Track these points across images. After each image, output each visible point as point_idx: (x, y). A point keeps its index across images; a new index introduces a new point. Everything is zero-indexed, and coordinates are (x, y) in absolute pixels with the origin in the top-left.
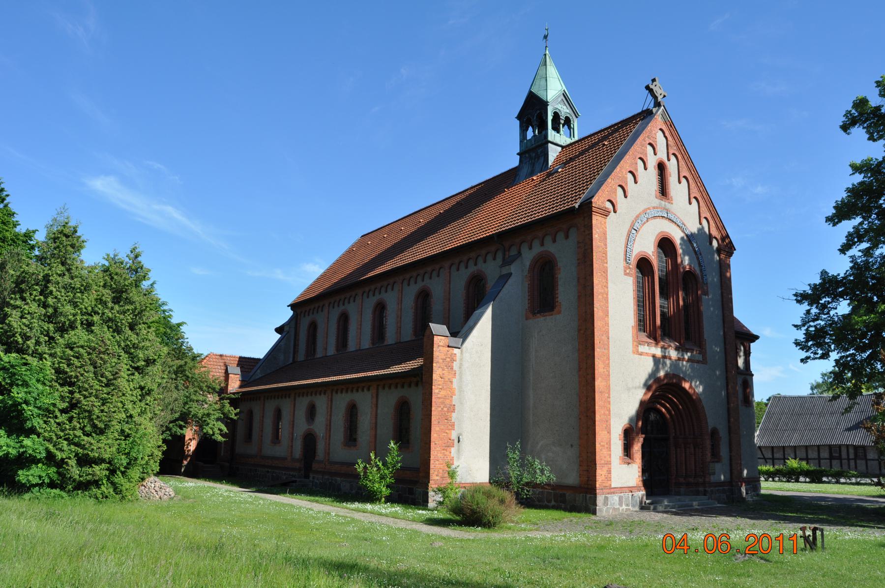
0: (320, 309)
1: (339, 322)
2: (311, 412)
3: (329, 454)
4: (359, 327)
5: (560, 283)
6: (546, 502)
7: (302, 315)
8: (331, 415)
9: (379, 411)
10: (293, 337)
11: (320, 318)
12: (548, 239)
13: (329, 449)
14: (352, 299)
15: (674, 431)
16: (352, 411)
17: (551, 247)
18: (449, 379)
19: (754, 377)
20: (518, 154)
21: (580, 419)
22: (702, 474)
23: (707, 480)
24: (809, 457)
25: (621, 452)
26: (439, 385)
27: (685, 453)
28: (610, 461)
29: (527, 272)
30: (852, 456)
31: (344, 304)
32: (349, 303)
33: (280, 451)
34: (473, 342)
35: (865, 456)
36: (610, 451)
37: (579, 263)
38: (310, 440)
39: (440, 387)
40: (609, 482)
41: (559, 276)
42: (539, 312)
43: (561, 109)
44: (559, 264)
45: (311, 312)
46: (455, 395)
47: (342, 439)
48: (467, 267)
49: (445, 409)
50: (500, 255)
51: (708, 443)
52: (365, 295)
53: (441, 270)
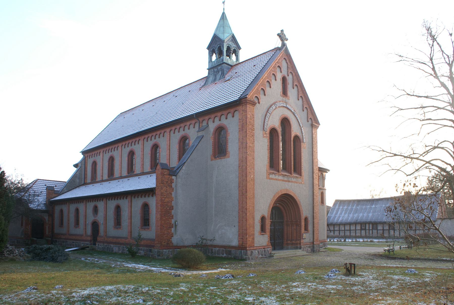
0: (98, 154)
1: (109, 161)
2: (96, 209)
3: (106, 232)
4: (120, 164)
5: (229, 141)
6: (221, 255)
7: (88, 157)
8: (106, 212)
9: (132, 210)
10: (83, 170)
11: (99, 159)
12: (223, 117)
13: (106, 230)
14: (116, 149)
15: (286, 218)
16: (118, 208)
17: (224, 122)
18: (170, 192)
19: (326, 191)
20: (207, 69)
21: (239, 212)
22: (299, 239)
23: (302, 242)
24: (351, 229)
25: (259, 229)
26: (164, 195)
27: (292, 228)
28: (254, 234)
29: (212, 135)
30: (371, 228)
31: (111, 152)
32: (114, 151)
33: (80, 231)
34: (182, 172)
35: (377, 229)
36: (254, 229)
37: (239, 131)
38: (95, 225)
39: (165, 197)
40: (253, 244)
41: (229, 137)
42: (218, 157)
43: (232, 45)
44: (229, 131)
45: (93, 156)
46: (173, 201)
47: (113, 225)
48: (179, 132)
49: (168, 208)
50: (197, 125)
51: (303, 223)
52: (123, 146)
53: (165, 133)
